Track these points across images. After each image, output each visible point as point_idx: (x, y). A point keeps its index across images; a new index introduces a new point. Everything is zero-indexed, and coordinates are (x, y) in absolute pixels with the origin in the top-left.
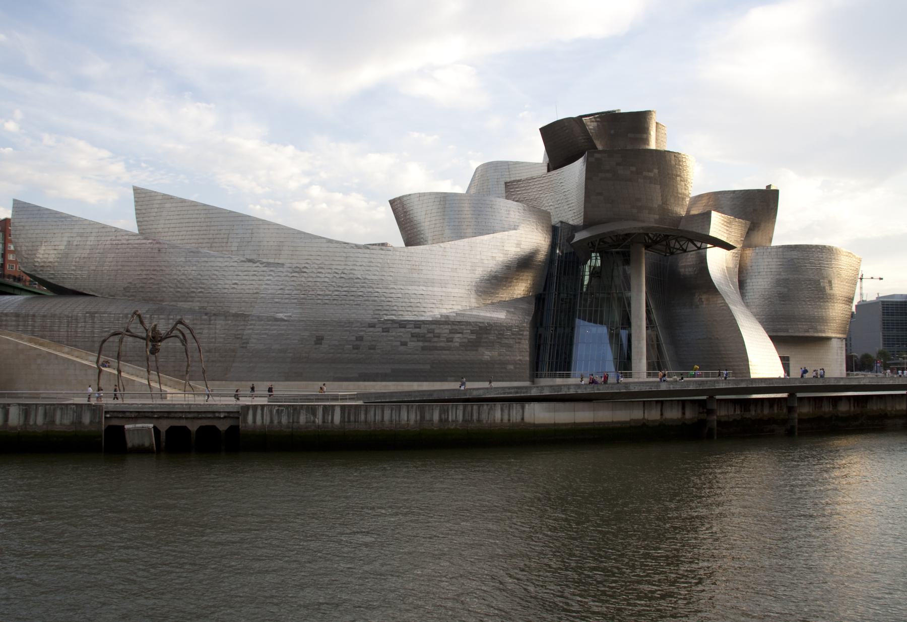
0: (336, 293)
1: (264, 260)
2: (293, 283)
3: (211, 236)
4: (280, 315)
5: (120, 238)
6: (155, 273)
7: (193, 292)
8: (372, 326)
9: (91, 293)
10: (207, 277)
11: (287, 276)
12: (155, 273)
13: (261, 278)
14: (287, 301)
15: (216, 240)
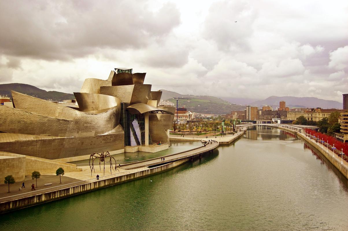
0: (86, 129)
1: (68, 120)
2: (76, 127)
3: (48, 111)
4: (73, 137)
5: (15, 111)
6: (31, 124)
7: (46, 131)
8: (94, 138)
9: (4, 132)
10: (50, 126)
11: (74, 124)
12: (31, 124)
13: (67, 125)
14: (74, 132)
15: (50, 113)
